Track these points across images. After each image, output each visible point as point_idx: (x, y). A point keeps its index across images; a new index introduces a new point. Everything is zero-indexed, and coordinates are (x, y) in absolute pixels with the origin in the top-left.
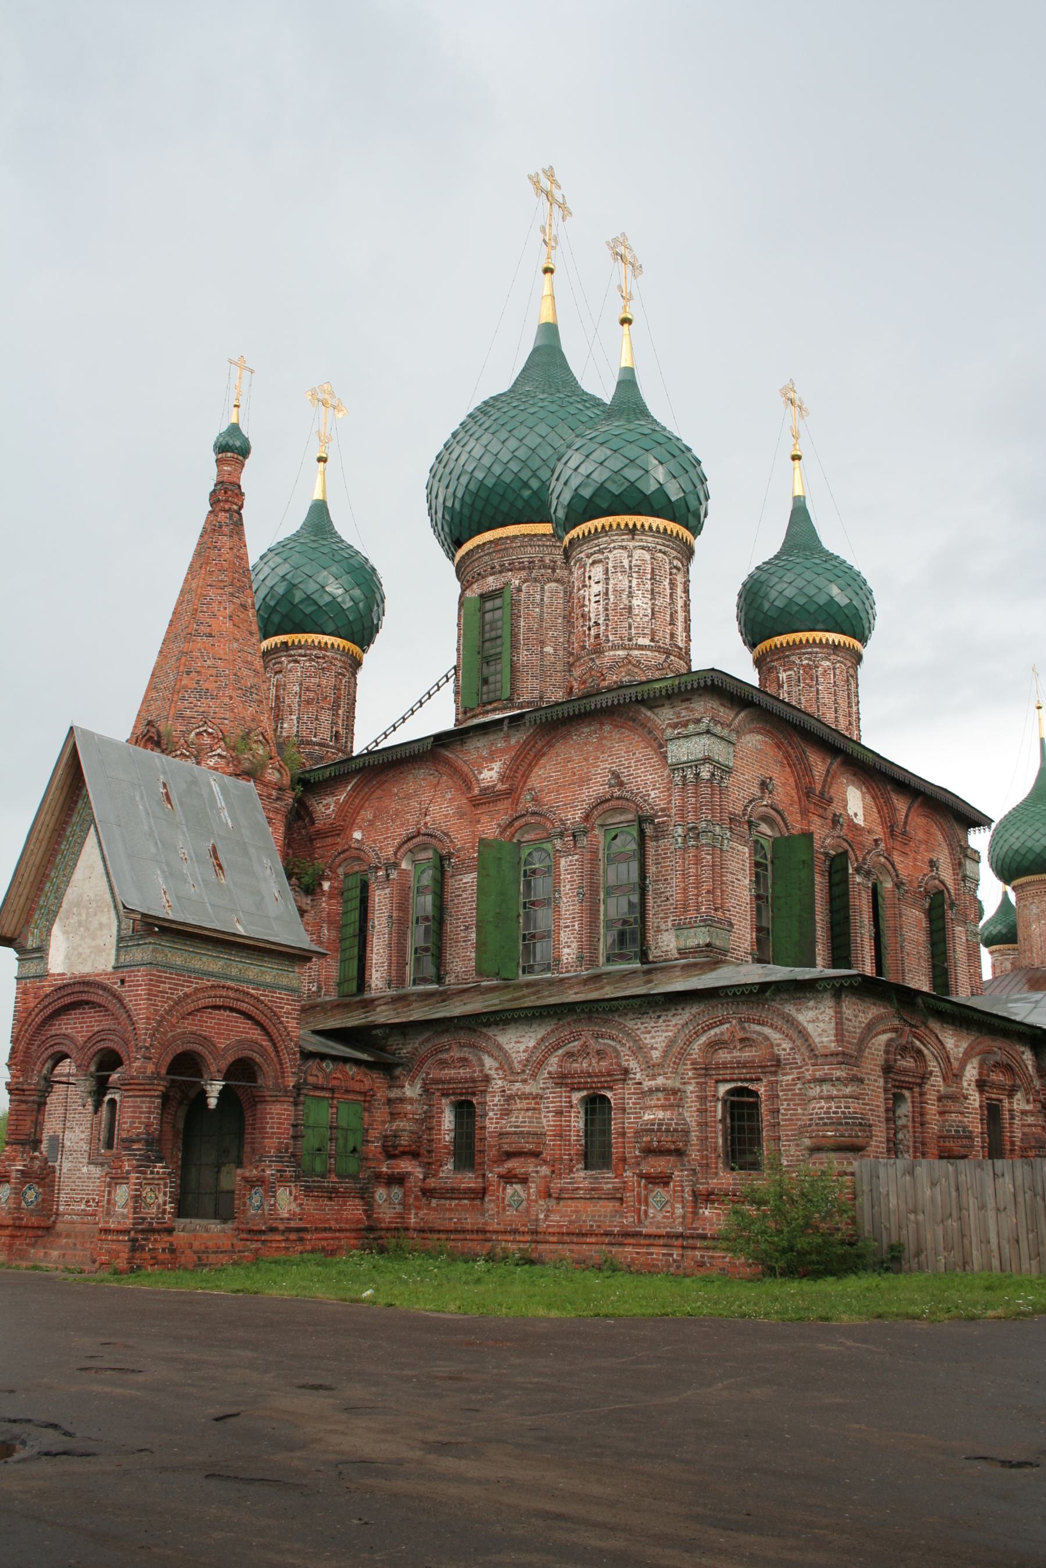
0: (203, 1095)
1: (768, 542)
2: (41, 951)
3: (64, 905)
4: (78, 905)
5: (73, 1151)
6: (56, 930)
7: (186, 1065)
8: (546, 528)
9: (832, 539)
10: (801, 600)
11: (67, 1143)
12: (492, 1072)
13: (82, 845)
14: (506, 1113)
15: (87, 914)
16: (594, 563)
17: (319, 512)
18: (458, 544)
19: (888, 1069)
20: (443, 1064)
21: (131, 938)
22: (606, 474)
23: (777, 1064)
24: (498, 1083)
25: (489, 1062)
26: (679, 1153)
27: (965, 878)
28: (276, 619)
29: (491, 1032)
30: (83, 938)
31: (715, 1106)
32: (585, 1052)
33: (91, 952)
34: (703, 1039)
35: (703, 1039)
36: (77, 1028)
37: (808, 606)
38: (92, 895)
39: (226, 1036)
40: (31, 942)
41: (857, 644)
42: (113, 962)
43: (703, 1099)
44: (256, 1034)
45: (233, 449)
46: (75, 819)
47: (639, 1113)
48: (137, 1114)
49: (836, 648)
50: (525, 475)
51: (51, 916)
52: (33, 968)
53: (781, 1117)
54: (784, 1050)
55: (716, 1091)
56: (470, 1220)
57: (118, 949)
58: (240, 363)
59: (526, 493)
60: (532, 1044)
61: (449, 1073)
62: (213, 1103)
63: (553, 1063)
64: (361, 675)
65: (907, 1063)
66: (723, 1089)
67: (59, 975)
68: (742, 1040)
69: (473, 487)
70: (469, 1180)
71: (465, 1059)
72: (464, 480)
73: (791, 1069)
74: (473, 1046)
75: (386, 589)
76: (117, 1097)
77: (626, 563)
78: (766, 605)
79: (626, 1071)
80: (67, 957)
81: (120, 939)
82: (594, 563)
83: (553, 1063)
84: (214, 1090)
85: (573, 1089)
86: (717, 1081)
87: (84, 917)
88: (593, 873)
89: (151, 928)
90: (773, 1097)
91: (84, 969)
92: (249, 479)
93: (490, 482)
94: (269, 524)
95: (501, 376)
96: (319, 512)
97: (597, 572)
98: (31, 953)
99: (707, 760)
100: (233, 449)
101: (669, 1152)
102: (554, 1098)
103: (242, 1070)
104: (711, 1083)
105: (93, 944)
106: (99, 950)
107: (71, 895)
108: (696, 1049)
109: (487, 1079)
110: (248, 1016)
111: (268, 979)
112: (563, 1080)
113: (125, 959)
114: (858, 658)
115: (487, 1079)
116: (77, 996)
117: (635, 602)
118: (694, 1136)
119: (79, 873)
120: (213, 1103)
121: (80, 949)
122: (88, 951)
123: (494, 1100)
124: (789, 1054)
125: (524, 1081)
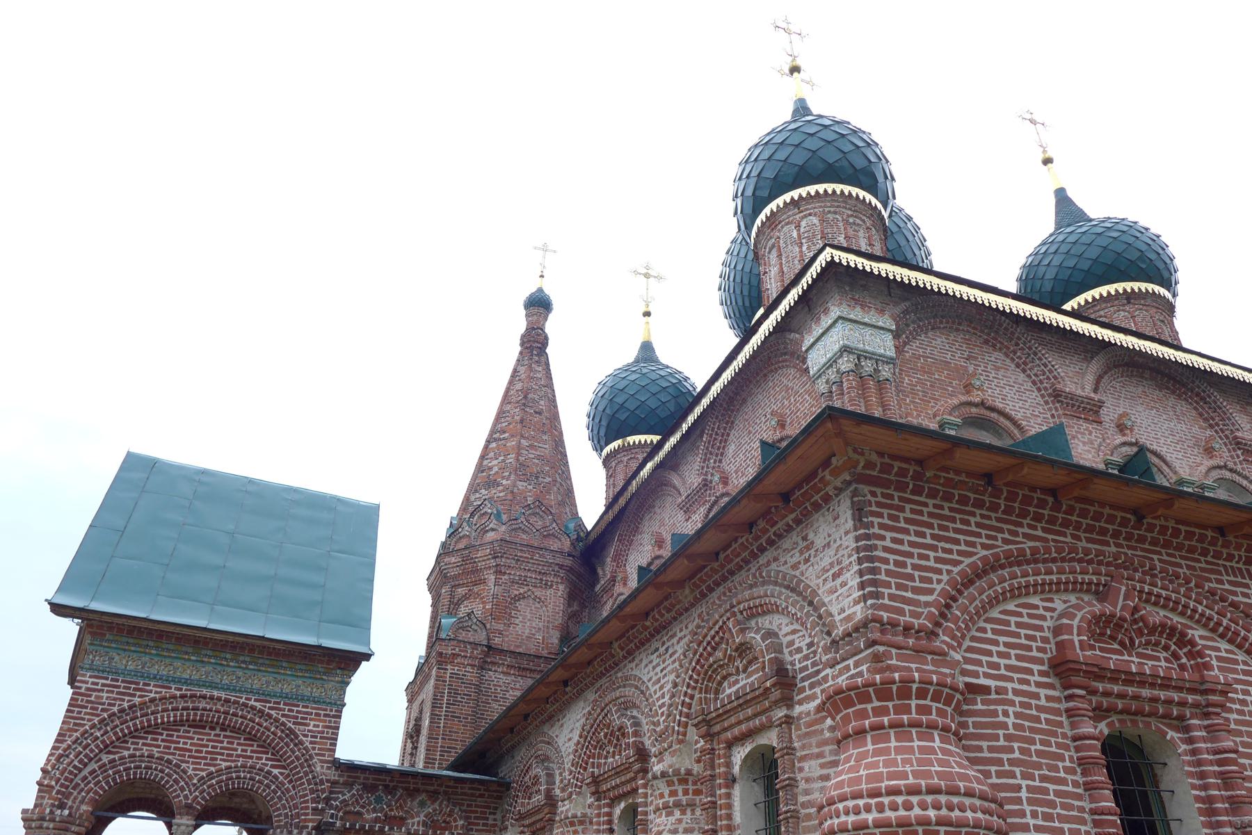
17: (647, 350)
19: (1063, 669)
31: (728, 796)
45: (539, 305)
53: (801, 799)
54: (799, 650)
55: (729, 765)
58: (545, 249)
66: (739, 755)
73: (812, 686)
77: (795, 234)
86: (730, 745)
96: (647, 350)
100: (539, 305)
104: (720, 748)
110: (251, 738)
115: (552, 802)
124: (806, 658)
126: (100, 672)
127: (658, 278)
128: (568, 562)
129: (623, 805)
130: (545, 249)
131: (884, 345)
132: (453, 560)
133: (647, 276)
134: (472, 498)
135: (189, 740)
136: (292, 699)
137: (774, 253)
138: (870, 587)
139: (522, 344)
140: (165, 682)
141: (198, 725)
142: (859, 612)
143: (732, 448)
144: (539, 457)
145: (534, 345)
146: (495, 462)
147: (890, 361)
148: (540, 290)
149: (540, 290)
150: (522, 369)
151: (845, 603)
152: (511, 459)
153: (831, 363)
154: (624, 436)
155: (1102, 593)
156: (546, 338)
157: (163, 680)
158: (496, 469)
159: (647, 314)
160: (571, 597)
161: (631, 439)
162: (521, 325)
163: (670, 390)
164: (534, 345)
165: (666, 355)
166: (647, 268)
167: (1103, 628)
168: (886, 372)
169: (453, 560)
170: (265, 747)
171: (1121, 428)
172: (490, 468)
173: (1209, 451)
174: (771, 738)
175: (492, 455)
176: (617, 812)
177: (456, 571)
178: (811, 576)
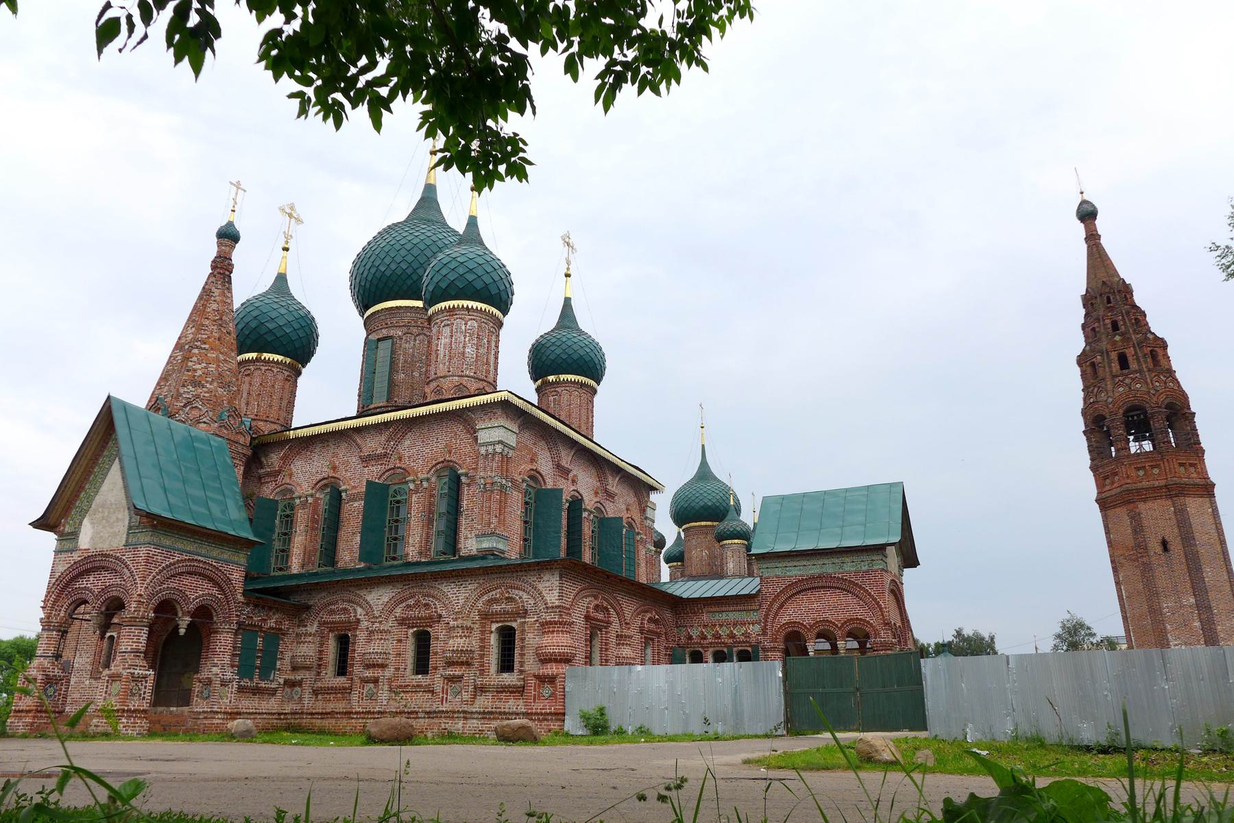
0: (177, 627)
1: (549, 322)
2: (74, 535)
4: (103, 506)
5: (79, 670)
6: (86, 522)
7: (166, 608)
8: (420, 304)
9: (585, 321)
10: (564, 357)
11: (76, 665)
12: (361, 618)
13: (109, 469)
14: (369, 640)
17: (281, 279)
18: (367, 308)
19: (587, 618)
20: (332, 612)
21: (138, 527)
22: (456, 276)
23: (525, 613)
24: (364, 624)
25: (359, 610)
26: (468, 664)
27: (646, 518)
28: (249, 342)
29: (362, 593)
30: (104, 527)
32: (417, 604)
34: (486, 598)
35: (486, 598)
36: (92, 583)
37: (568, 360)
39: (197, 591)
40: (68, 529)
41: (592, 383)
43: (483, 632)
44: (215, 591)
45: (228, 236)
46: (106, 453)
47: (446, 643)
48: (132, 640)
49: (582, 385)
50: (409, 271)
51: (83, 514)
52: (68, 545)
56: (340, 706)
57: (128, 534)
58: (238, 186)
59: (409, 282)
61: (337, 618)
62: (182, 631)
63: (398, 611)
64: (300, 380)
65: (600, 616)
66: (494, 627)
68: (507, 598)
69: (378, 275)
70: (341, 681)
71: (345, 609)
72: (373, 270)
74: (350, 601)
75: (320, 331)
76: (115, 634)
78: (544, 358)
79: (440, 616)
80: (92, 539)
81: (130, 528)
83: (398, 611)
84: (184, 623)
85: (409, 627)
88: (430, 504)
89: (152, 523)
90: (523, 631)
91: (105, 547)
92: (239, 255)
93: (388, 273)
94: (248, 284)
95: (401, 213)
96: (281, 279)
97: (447, 331)
98: (67, 539)
99: (500, 442)
100: (228, 236)
101: (462, 663)
102: (398, 632)
103: (203, 614)
106: (115, 535)
107: (98, 499)
108: (480, 604)
109: (358, 621)
110: (211, 579)
111: (225, 557)
112: (402, 622)
113: (132, 540)
114: (595, 392)
115: (358, 621)
116: (93, 564)
117: (467, 350)
118: (476, 655)
119: (105, 487)
120: (182, 631)
123: (361, 636)
125: (380, 622)
126: (157, 546)
127: (299, 221)
128: (249, 453)
130: (238, 186)
131: (512, 440)
133: (290, 216)
134: (182, 391)
135: (187, 580)
136: (227, 562)
137: (447, 331)
138: (561, 597)
139: (213, 268)
140: (182, 552)
141: (190, 573)
142: (557, 603)
143: (407, 443)
144: (229, 370)
145: (222, 268)
146: (198, 366)
147: (513, 448)
148: (230, 224)
149: (230, 224)
150: (217, 292)
151: (552, 598)
152: (212, 367)
153: (493, 444)
154: (260, 350)
155: (596, 598)
156: (232, 266)
157: (183, 551)
158: (199, 373)
159: (286, 249)
160: (246, 474)
161: (266, 356)
162: (211, 250)
163: (307, 329)
164: (222, 268)
165: (297, 290)
166: (292, 208)
167: (597, 607)
168: (511, 453)
170: (216, 584)
171: (573, 482)
172: (195, 370)
173: (596, 493)
174: (514, 625)
175: (195, 359)
178: (540, 586)
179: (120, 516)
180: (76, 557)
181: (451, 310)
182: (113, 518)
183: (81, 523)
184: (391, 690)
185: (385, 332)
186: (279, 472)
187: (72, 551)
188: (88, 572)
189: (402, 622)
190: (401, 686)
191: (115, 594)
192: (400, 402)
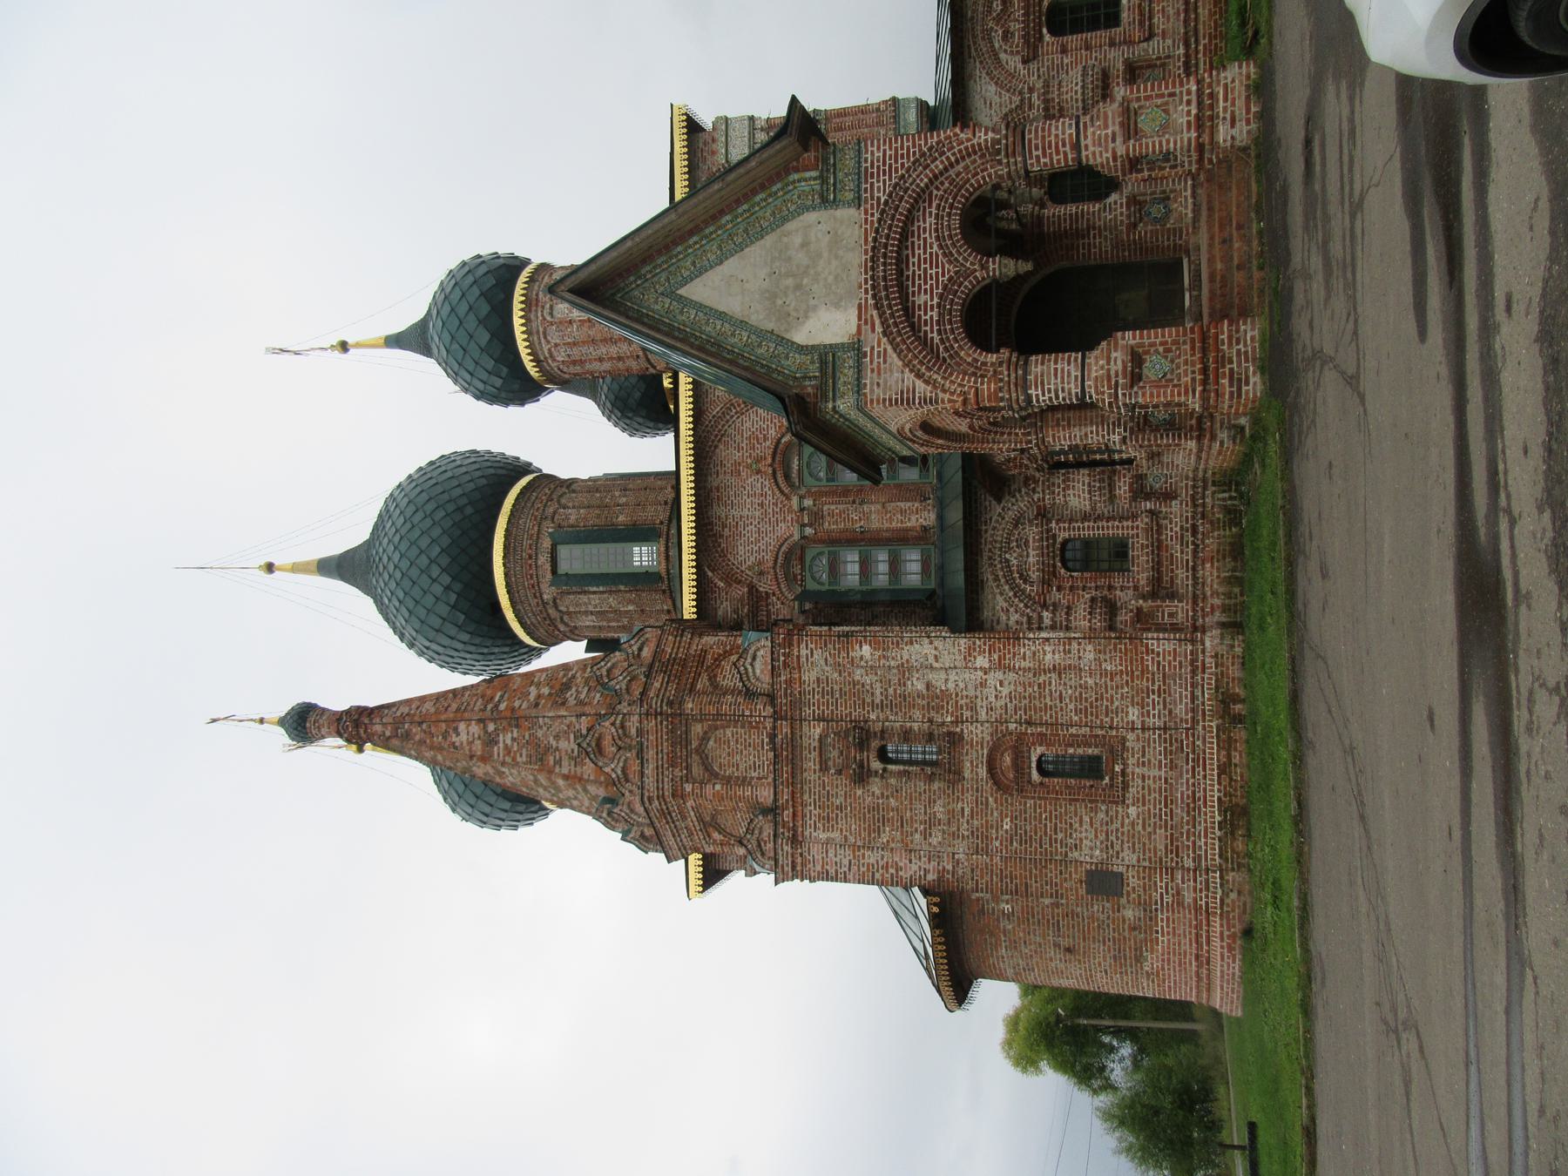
2: (827, 357)
3: (770, 326)
6: (801, 337)
13: (700, 307)
15: (787, 275)
16: (551, 314)
33: (836, 257)
38: (763, 273)
42: (852, 211)
45: (304, 723)
57: (835, 204)
60: (993, 88)
67: (860, 319)
80: (837, 305)
82: (551, 314)
83: (1013, 62)
87: (790, 282)
100: (304, 723)
105: (826, 255)
107: (760, 318)
119: (732, 304)
121: (831, 279)
122: (834, 263)
125: (1031, 90)
129: (1045, 30)
132: (657, 685)
145: (358, 726)
148: (282, 722)
149: (282, 722)
164: (358, 726)
169: (657, 685)
172: (539, 696)
176: (1047, 37)
177: (672, 688)
179: (798, 240)
180: (875, 340)
181: (529, 304)
182: (801, 258)
183: (802, 349)
184: (1147, 40)
185: (544, 559)
186: (752, 587)
187: (860, 354)
188: (908, 311)
189: (1031, 54)
190: (1141, 23)
191: (956, 222)
192: (663, 514)
